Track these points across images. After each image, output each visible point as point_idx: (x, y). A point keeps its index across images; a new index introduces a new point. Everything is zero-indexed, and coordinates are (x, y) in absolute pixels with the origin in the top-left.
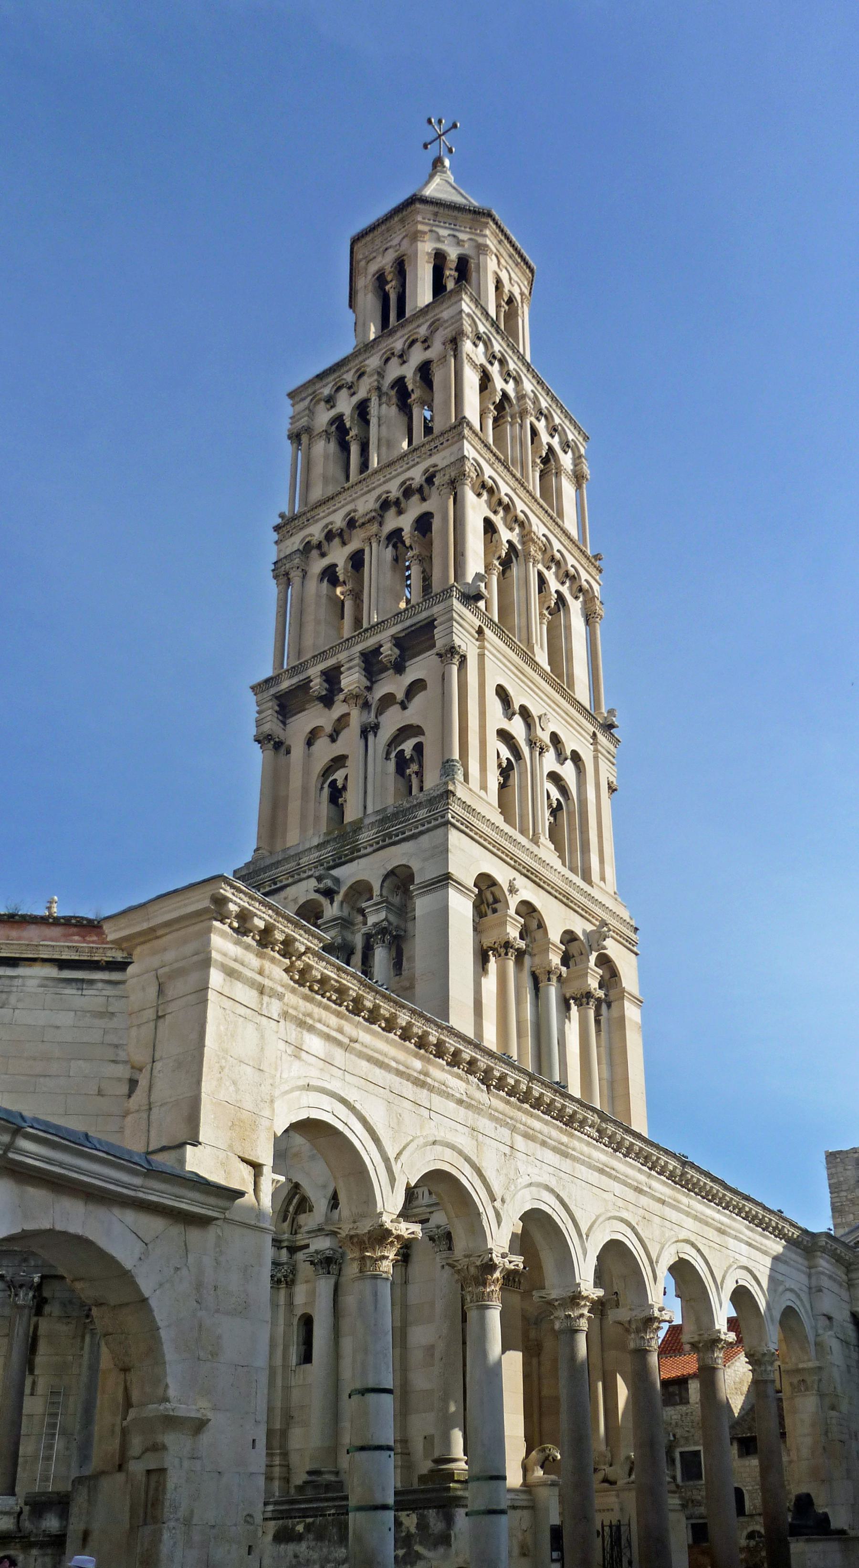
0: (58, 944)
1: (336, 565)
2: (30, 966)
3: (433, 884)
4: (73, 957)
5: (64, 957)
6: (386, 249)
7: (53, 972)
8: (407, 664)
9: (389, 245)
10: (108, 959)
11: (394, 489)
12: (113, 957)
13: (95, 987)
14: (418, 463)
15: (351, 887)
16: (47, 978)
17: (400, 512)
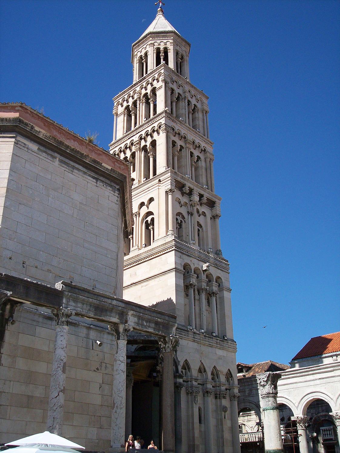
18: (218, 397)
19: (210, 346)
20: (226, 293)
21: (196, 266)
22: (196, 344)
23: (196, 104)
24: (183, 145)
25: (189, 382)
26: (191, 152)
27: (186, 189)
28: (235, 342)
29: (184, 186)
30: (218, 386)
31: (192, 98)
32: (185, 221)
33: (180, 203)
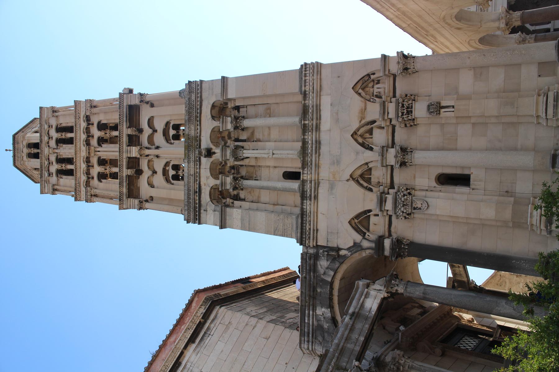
0: (180, 336)
1: (99, 173)
2: (185, 356)
3: (224, 87)
4: (191, 333)
5: (189, 337)
6: (22, 151)
7: (193, 346)
8: (141, 127)
9: (21, 150)
10: (201, 317)
11: (84, 137)
12: (202, 313)
13: (212, 328)
14: (80, 124)
15: (212, 142)
16: (194, 350)
17: (93, 136)
18: (412, 124)
19: (320, 148)
20: (231, 94)
21: (209, 174)
22: (321, 191)
23: (54, 127)
24: (94, 161)
25: (390, 213)
26: (99, 145)
27: (130, 172)
28: (302, 66)
29: (129, 177)
30: (391, 121)
31: (52, 138)
32: (171, 161)
33: (153, 175)
